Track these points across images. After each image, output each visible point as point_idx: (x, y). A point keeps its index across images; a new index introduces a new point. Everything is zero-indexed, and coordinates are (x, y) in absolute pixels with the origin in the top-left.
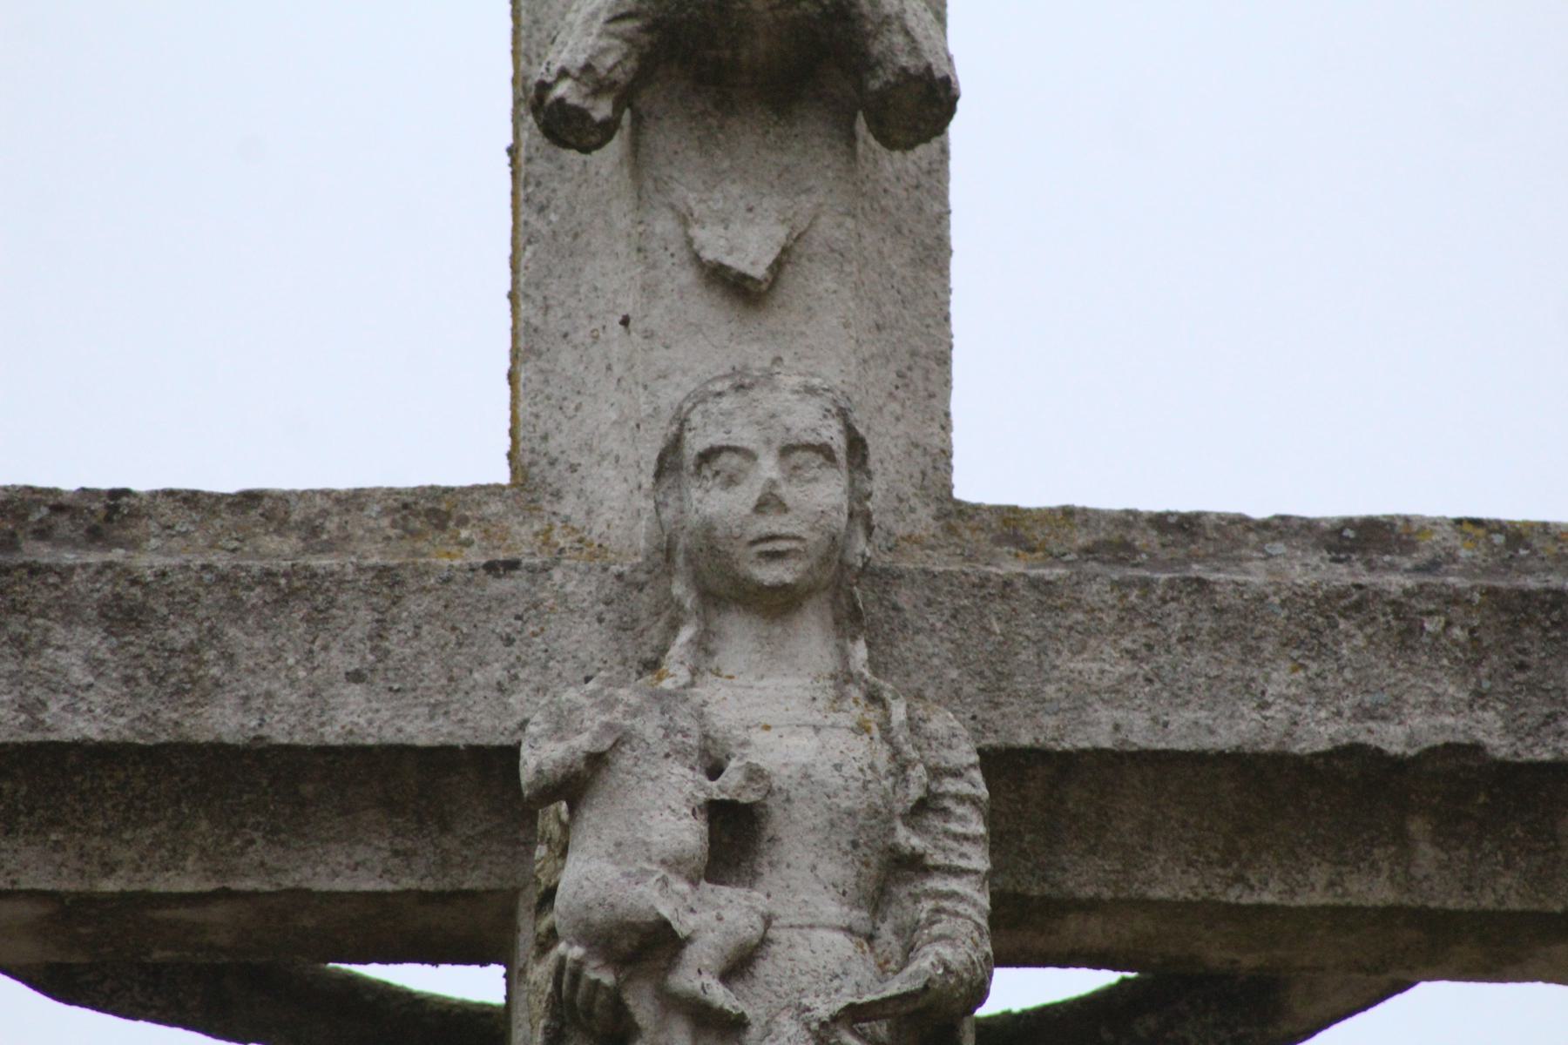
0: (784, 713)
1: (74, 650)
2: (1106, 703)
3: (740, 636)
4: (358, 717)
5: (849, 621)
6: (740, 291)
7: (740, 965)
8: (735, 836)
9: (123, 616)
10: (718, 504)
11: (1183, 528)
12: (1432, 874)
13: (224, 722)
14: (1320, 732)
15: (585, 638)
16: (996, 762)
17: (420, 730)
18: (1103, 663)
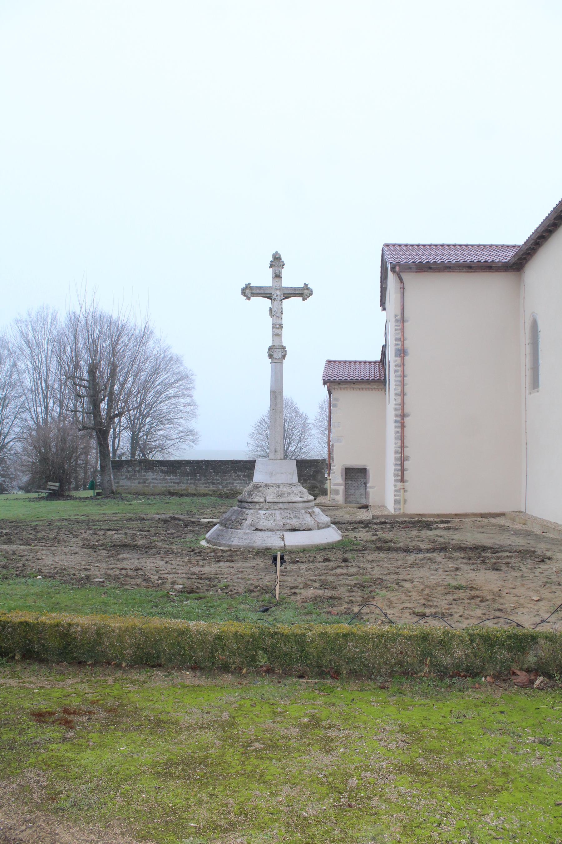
0: (278, 293)
2: (286, 292)
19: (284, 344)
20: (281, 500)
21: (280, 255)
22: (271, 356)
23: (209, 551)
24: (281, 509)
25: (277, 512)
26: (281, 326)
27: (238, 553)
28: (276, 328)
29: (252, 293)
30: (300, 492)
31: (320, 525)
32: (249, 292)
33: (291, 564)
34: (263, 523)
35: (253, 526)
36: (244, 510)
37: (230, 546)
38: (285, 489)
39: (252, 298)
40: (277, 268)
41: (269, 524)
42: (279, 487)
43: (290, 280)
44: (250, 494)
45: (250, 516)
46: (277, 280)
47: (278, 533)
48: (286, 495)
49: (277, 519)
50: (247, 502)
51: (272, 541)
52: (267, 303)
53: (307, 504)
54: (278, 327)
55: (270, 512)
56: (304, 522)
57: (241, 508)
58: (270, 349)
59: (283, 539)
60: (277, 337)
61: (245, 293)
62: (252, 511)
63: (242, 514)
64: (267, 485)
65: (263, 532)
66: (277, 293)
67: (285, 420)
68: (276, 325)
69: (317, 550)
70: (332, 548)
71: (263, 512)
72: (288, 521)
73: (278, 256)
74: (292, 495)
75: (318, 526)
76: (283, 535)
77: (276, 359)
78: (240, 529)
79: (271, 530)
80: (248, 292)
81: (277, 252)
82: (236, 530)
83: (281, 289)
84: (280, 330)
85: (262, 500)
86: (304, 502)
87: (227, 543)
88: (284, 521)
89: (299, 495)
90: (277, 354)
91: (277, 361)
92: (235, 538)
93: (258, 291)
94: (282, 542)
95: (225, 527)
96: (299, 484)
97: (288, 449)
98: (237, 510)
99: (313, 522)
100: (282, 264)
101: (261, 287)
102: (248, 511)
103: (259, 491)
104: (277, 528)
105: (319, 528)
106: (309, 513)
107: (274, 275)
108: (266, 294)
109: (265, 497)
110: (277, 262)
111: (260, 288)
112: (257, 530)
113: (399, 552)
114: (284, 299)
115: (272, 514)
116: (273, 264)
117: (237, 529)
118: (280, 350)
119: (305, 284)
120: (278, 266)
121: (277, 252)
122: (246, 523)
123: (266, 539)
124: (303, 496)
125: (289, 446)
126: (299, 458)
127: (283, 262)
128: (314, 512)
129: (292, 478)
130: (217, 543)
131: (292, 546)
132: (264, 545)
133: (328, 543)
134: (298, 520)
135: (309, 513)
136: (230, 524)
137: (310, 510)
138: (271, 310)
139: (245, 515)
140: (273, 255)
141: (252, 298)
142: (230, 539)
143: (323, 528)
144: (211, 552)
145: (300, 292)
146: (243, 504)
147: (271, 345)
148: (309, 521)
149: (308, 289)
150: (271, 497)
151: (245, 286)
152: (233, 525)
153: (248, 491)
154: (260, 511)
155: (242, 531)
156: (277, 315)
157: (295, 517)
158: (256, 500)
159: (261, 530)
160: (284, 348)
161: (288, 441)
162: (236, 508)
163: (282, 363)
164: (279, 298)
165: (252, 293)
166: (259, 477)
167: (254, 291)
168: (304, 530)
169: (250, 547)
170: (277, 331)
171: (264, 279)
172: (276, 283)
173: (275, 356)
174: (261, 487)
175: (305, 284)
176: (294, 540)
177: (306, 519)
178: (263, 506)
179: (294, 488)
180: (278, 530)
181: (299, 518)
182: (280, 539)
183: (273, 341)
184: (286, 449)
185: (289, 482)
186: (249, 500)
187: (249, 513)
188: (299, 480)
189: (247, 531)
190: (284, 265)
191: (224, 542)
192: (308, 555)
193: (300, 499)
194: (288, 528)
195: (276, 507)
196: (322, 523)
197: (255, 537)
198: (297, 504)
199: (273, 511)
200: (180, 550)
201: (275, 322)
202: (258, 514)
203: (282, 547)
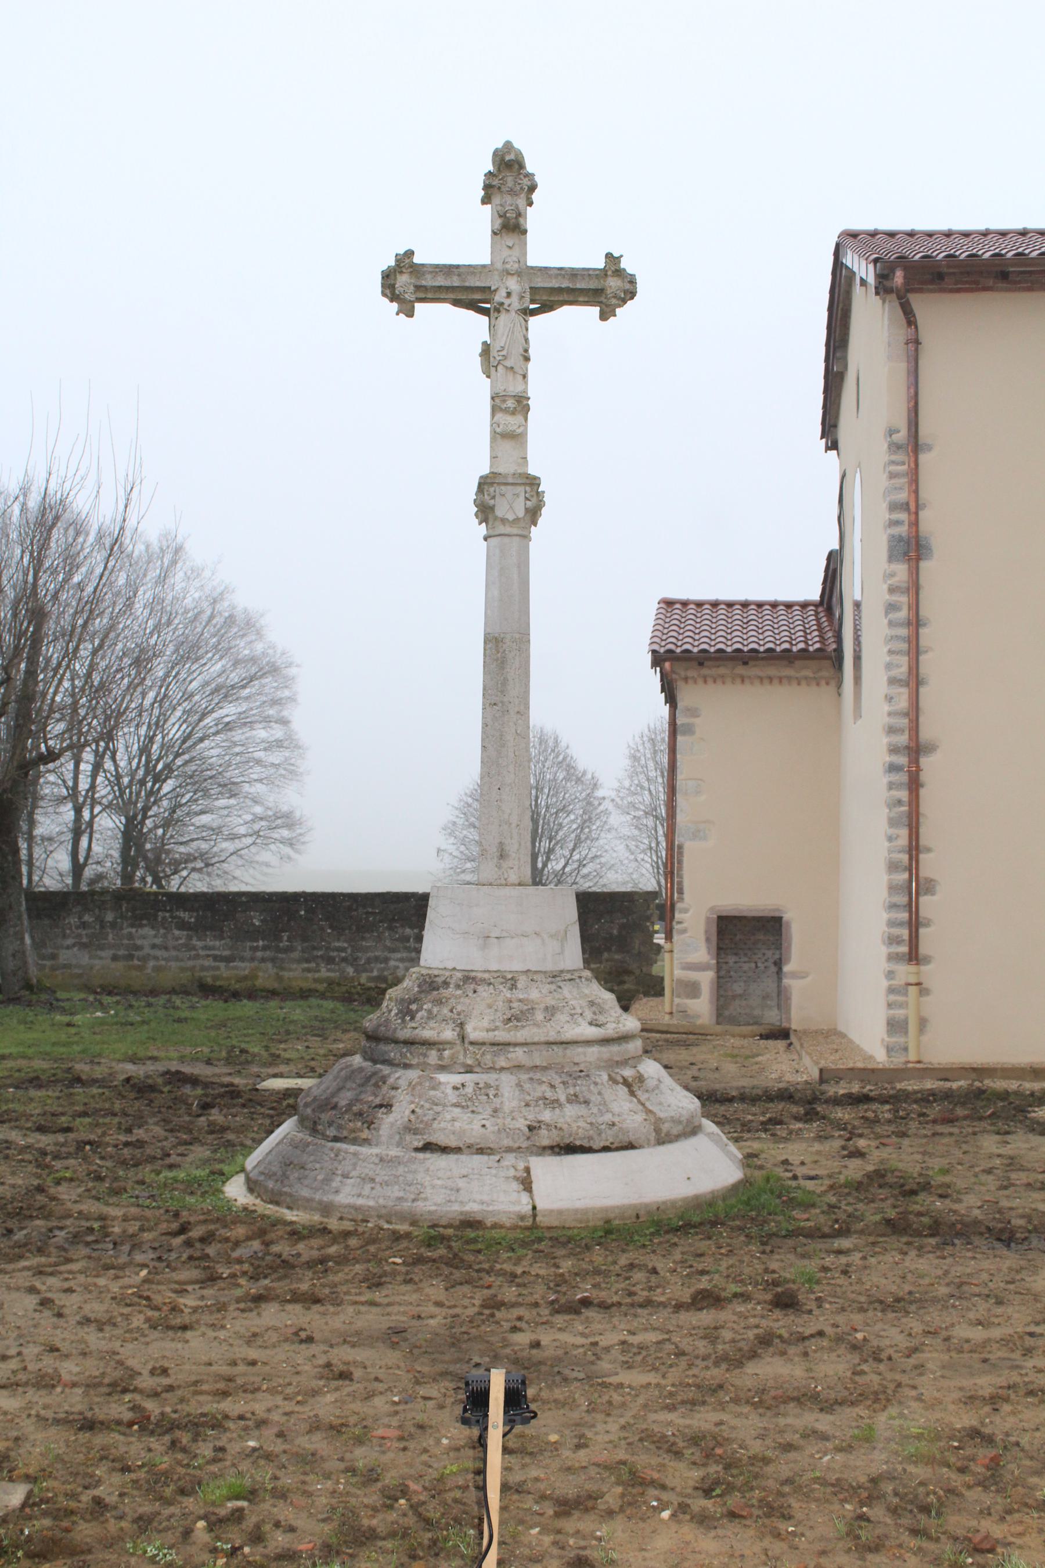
0: (513, 284)
1: (455, 278)
2: (540, 283)
4: (478, 284)
8: (509, 295)
10: (508, 266)
12: (566, 297)
13: (467, 284)
15: (496, 277)
19: (532, 470)
20: (521, 1036)
21: (519, 154)
22: (485, 512)
23: (240, 1231)
24: (519, 1067)
25: (507, 1081)
26: (522, 405)
27: (353, 1242)
28: (506, 411)
29: (418, 288)
30: (592, 1003)
31: (665, 1127)
32: (410, 284)
33: (560, 1320)
34: (455, 1124)
35: (416, 1132)
36: (386, 1070)
37: (326, 1209)
38: (534, 994)
39: (418, 306)
40: (509, 199)
41: (476, 1126)
42: (514, 987)
43: (555, 240)
44: (407, 1012)
45: (406, 1093)
46: (510, 240)
47: (510, 1159)
48: (539, 1016)
49: (507, 1108)
50: (396, 1042)
51: (484, 1191)
52: (473, 327)
53: (615, 1048)
54: (511, 407)
55: (482, 1078)
56: (608, 1117)
57: (375, 1062)
58: (484, 484)
59: (527, 1184)
60: (507, 446)
61: (392, 287)
62: (413, 1074)
63: (376, 1085)
64: (469, 979)
65: (452, 1157)
66: (508, 286)
67: (539, 789)
68: (504, 398)
69: (657, 1233)
70: (714, 1224)
71: (456, 1079)
72: (547, 1116)
73: (512, 157)
74: (562, 1017)
75: (657, 1131)
76: (527, 1170)
77: (504, 521)
78: (366, 1142)
79: (481, 1151)
80: (403, 281)
81: (508, 145)
82: (353, 1148)
83: (526, 272)
84: (519, 418)
85: (449, 1034)
86: (606, 1041)
87: (317, 1197)
88: (531, 1115)
89: (588, 1015)
90: (508, 502)
91: (508, 530)
92: (346, 1176)
93: (441, 281)
94: (525, 1198)
95: (314, 1131)
96: (588, 973)
97: (545, 865)
98: (361, 1069)
99: (640, 1117)
100: (526, 182)
101: (451, 267)
102: (400, 1073)
103: (439, 1002)
104: (507, 1142)
105: (663, 1139)
106: (626, 1083)
107: (499, 221)
108: (466, 290)
109: (462, 1025)
110: (508, 180)
111: (449, 270)
112: (428, 1147)
113: (977, 1240)
114: (533, 313)
115: (488, 1086)
116: (496, 182)
117: (355, 1141)
118: (520, 490)
119: (609, 256)
120: (512, 192)
121: (508, 145)
122: (389, 1123)
123: (461, 1183)
124: (602, 1019)
125: (548, 859)
126: (586, 885)
127: (530, 176)
128: (641, 1079)
129: (562, 953)
130: (281, 1193)
131: (560, 1212)
132: (456, 1207)
133: (696, 1197)
134: (582, 1110)
135: (626, 1083)
136: (330, 1124)
137: (628, 1073)
138: (486, 351)
139: (385, 1089)
140: (496, 153)
141: (418, 306)
142: (327, 1180)
143: (677, 1138)
144: (249, 1238)
145: (593, 285)
146: (383, 1047)
147: (486, 470)
148: (623, 1111)
149: (619, 273)
150: (485, 1023)
151: (393, 263)
152: (340, 1127)
153: (403, 1000)
154: (443, 1077)
155: (375, 1150)
156: (508, 364)
157: (573, 1099)
158: (427, 1034)
159: (445, 1150)
160: (533, 482)
161: (545, 844)
162: (357, 1060)
163: (526, 537)
164: (515, 303)
165: (418, 288)
166: (441, 948)
167: (428, 281)
168: (606, 1149)
169: (402, 1217)
170: (511, 422)
171: (463, 238)
172: (506, 252)
173: (499, 512)
174: (446, 984)
175: (609, 256)
176: (571, 1188)
177: (615, 1107)
178: (452, 1057)
179: (567, 991)
180: (509, 1150)
181: (587, 1102)
182: (515, 1186)
183: (494, 458)
184: (540, 865)
185: (549, 966)
186: (404, 1034)
187: (403, 1083)
188: (587, 962)
189: (394, 1152)
190: (532, 188)
191: (305, 1193)
192: (623, 1261)
193: (592, 1032)
194: (546, 1142)
195: (502, 1062)
196: (673, 1120)
197: (420, 1177)
198: (580, 1050)
199: (491, 1078)
200: (133, 1227)
201: (500, 388)
202: (436, 1086)
203: (522, 1218)
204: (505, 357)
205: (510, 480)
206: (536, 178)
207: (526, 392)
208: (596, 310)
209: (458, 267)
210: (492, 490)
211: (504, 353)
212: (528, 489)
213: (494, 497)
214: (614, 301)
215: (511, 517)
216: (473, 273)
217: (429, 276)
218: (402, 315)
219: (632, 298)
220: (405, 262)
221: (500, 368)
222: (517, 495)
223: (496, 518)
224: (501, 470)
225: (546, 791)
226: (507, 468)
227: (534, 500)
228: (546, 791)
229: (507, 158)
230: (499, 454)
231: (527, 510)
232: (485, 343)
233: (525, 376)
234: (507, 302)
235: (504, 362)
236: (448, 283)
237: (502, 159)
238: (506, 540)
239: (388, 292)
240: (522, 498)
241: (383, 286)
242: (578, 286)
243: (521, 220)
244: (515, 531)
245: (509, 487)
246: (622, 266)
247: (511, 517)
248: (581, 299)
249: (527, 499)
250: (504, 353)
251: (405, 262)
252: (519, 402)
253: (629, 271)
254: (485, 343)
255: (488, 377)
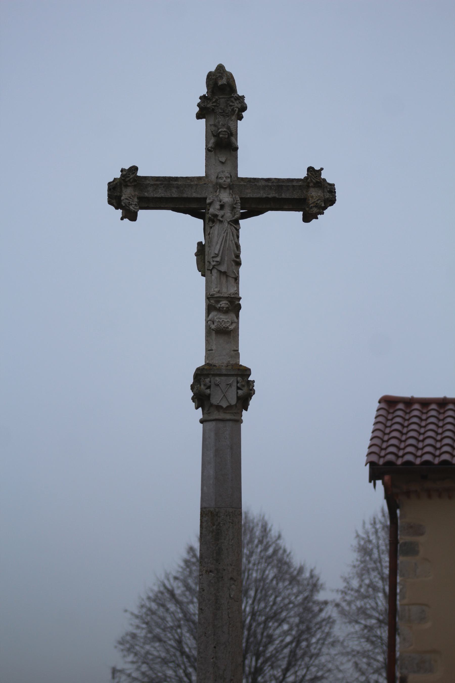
0: (226, 197)
1: (174, 190)
2: (249, 194)
3: (222, 191)
4: (194, 195)
5: (230, 189)
6: (222, 163)
7: (222, 217)
8: (222, 207)
9: (178, 187)
10: (221, 181)
11: (255, 179)
13: (185, 196)
14: (265, 196)
15: (211, 189)
16: (241, 199)
17: (199, 196)
18: (249, 191)
19: (244, 361)
21: (230, 78)
22: (201, 399)
26: (234, 305)
28: (220, 310)
32: (132, 193)
39: (141, 213)
40: (221, 120)
43: (262, 155)
52: (189, 230)
54: (223, 309)
58: (200, 375)
68: (218, 299)
73: (223, 81)
77: (219, 408)
80: (127, 193)
81: (220, 68)
90: (222, 391)
91: (222, 416)
93: (161, 193)
100: (237, 105)
107: (212, 140)
110: (221, 102)
114: (244, 216)
118: (232, 380)
119: (310, 170)
120: (224, 114)
121: (220, 68)
140: (210, 75)
141: (141, 213)
145: (296, 195)
147: (201, 362)
151: (118, 175)
156: (223, 268)
160: (245, 372)
164: (228, 214)
167: (150, 193)
170: (223, 319)
171: (183, 153)
172: (220, 168)
173: (215, 400)
175: (310, 170)
183: (208, 350)
190: (244, 108)
201: (214, 290)
204: (219, 263)
205: (224, 372)
206: (246, 101)
207: (238, 293)
208: (299, 215)
209: (176, 179)
210: (208, 380)
211: (218, 259)
212: (239, 379)
213: (209, 387)
214: (315, 210)
215: (224, 404)
216: (190, 186)
217: (151, 189)
218: (126, 220)
219: (332, 205)
220: (129, 177)
221: (214, 271)
222: (230, 385)
223: (211, 405)
224: (216, 361)
225: (252, 593)
226: (220, 361)
227: (245, 389)
228: (252, 593)
229: (220, 83)
230: (214, 348)
231: (238, 398)
232: (200, 244)
233: (236, 279)
234: (221, 213)
235: (219, 264)
236: (168, 195)
237: (216, 84)
238: (221, 425)
239: (114, 201)
240: (234, 388)
241: (110, 196)
242: (283, 196)
243: (233, 139)
244: (228, 417)
245: (223, 378)
246: (322, 177)
247: (224, 404)
248: (286, 207)
249: (238, 388)
250: (218, 259)
251: (129, 177)
252: (230, 302)
253: (329, 181)
254: (200, 244)
255: (203, 275)
